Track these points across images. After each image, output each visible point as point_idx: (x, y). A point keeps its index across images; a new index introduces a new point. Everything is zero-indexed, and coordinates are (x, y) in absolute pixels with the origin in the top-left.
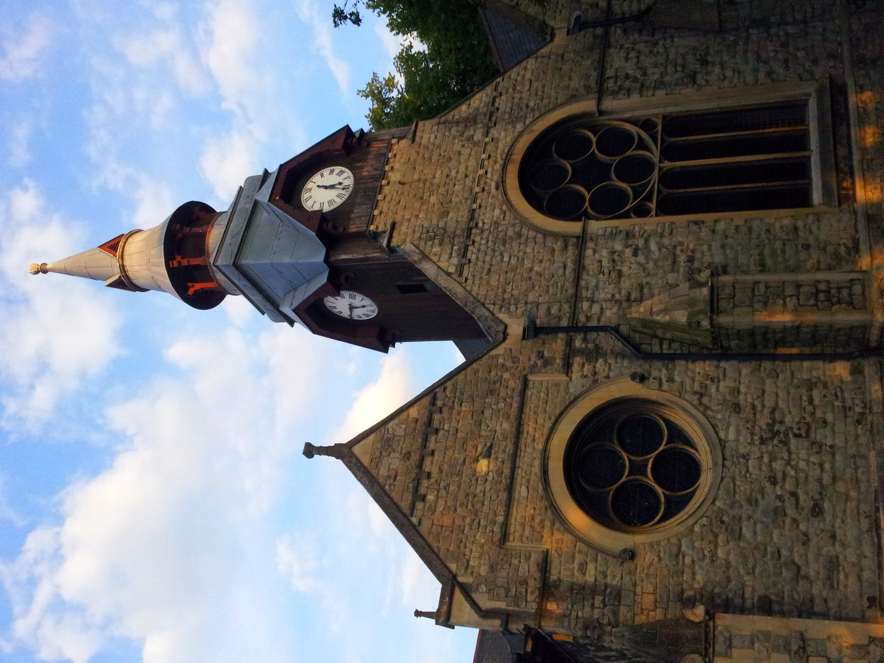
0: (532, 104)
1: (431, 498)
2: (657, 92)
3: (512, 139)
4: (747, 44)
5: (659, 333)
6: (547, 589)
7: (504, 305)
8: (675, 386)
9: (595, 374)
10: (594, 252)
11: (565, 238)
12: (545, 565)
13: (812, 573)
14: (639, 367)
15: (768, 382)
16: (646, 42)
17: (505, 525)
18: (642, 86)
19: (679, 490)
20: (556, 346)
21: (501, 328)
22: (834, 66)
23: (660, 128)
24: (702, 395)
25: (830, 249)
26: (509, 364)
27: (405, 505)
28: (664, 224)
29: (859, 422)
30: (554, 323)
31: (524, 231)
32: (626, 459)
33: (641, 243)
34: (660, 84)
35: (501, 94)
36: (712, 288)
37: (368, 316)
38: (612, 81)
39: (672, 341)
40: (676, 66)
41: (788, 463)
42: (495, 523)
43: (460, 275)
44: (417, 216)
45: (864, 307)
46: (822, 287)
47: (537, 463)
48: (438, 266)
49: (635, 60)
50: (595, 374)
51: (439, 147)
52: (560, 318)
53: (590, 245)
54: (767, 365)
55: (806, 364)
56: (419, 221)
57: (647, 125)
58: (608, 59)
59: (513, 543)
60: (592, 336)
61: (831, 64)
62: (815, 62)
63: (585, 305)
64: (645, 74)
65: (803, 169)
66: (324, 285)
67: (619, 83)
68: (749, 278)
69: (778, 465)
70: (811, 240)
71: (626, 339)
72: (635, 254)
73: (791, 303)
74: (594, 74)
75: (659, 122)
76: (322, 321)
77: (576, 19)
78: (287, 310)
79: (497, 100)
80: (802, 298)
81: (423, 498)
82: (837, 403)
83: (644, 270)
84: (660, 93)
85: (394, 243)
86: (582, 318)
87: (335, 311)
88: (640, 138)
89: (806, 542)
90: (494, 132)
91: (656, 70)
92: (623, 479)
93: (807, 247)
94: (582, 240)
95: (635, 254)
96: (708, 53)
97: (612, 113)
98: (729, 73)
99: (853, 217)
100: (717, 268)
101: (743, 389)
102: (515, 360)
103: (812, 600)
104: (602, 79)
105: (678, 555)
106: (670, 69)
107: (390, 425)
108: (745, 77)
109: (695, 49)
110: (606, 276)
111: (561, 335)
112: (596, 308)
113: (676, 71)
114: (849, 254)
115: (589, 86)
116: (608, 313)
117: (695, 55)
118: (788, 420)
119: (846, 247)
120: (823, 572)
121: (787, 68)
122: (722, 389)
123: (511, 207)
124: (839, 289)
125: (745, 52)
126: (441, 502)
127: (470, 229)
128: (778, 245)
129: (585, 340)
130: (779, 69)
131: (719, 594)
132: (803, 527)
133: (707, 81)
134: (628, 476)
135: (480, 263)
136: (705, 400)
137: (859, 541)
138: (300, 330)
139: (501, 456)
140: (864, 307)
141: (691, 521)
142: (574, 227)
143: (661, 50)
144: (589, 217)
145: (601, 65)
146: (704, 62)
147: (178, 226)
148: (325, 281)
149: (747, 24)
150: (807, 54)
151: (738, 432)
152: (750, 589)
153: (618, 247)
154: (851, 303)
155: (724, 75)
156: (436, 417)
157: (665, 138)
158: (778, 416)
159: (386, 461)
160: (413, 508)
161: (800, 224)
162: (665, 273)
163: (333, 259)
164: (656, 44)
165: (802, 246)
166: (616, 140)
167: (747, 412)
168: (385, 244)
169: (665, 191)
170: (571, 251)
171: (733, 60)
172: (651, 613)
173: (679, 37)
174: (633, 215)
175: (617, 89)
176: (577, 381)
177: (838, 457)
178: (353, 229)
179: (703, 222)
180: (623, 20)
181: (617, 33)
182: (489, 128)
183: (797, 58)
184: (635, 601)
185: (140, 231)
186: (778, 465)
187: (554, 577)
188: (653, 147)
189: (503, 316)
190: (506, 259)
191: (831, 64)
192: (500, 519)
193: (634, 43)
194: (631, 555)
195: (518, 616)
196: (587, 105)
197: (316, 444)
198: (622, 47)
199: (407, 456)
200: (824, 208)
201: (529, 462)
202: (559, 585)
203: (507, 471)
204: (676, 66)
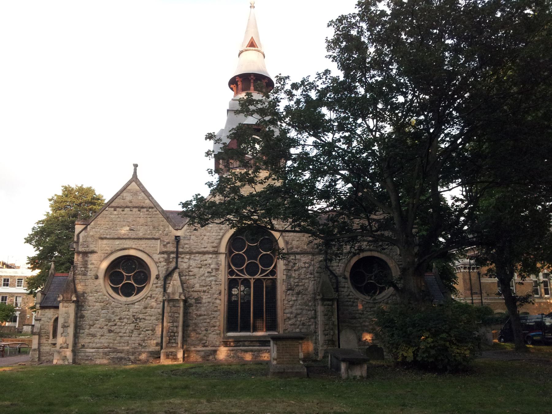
1: (115, 212)
6: (85, 254)
8: (154, 289)
9: (160, 262)
10: (211, 258)
11: (218, 246)
12: (93, 252)
13: (91, 330)
14: (162, 276)
15: (155, 318)
17: (106, 238)
20: (171, 248)
23: (271, 277)
24: (151, 297)
25: (205, 338)
26: (165, 232)
27: (113, 204)
29: (139, 344)
30: (180, 246)
31: (223, 231)
33: (213, 274)
34: (289, 277)
38: (294, 258)
41: (126, 323)
42: (107, 235)
46: (176, 334)
47: (127, 246)
50: (160, 262)
52: (183, 248)
53: (214, 256)
57: (273, 272)
59: (100, 242)
60: (175, 260)
63: (188, 257)
64: (295, 271)
69: (125, 320)
70: (209, 332)
72: (208, 272)
73: (170, 325)
75: (274, 277)
80: (172, 328)
81: (115, 210)
82: (146, 338)
84: (285, 277)
86: (183, 256)
88: (267, 270)
93: (207, 330)
94: (216, 253)
95: (208, 272)
98: (291, 303)
101: (152, 310)
102: (167, 235)
103: (83, 329)
105: (97, 292)
106: (296, 280)
107: (143, 194)
109: (307, 289)
111: (175, 250)
112: (186, 260)
116: (184, 265)
118: (140, 323)
120: (91, 333)
121: (291, 325)
122: (153, 303)
126: (113, 216)
128: (208, 320)
129: (173, 258)
132: (105, 327)
133: (289, 294)
136: (149, 298)
137: (101, 343)
139: (130, 234)
141: (107, 295)
142: (223, 248)
143: (307, 277)
146: (298, 293)
151: (137, 308)
153: (212, 266)
154: (169, 343)
156: (145, 210)
159: (129, 195)
160: (112, 207)
161: (216, 328)
164: (311, 274)
166: (268, 261)
167: (144, 311)
170: (211, 249)
176: (156, 257)
177: (128, 338)
186: (125, 320)
187: (89, 255)
192: (108, 237)
194: (97, 278)
195: (78, 246)
199: (131, 202)
203: (125, 237)
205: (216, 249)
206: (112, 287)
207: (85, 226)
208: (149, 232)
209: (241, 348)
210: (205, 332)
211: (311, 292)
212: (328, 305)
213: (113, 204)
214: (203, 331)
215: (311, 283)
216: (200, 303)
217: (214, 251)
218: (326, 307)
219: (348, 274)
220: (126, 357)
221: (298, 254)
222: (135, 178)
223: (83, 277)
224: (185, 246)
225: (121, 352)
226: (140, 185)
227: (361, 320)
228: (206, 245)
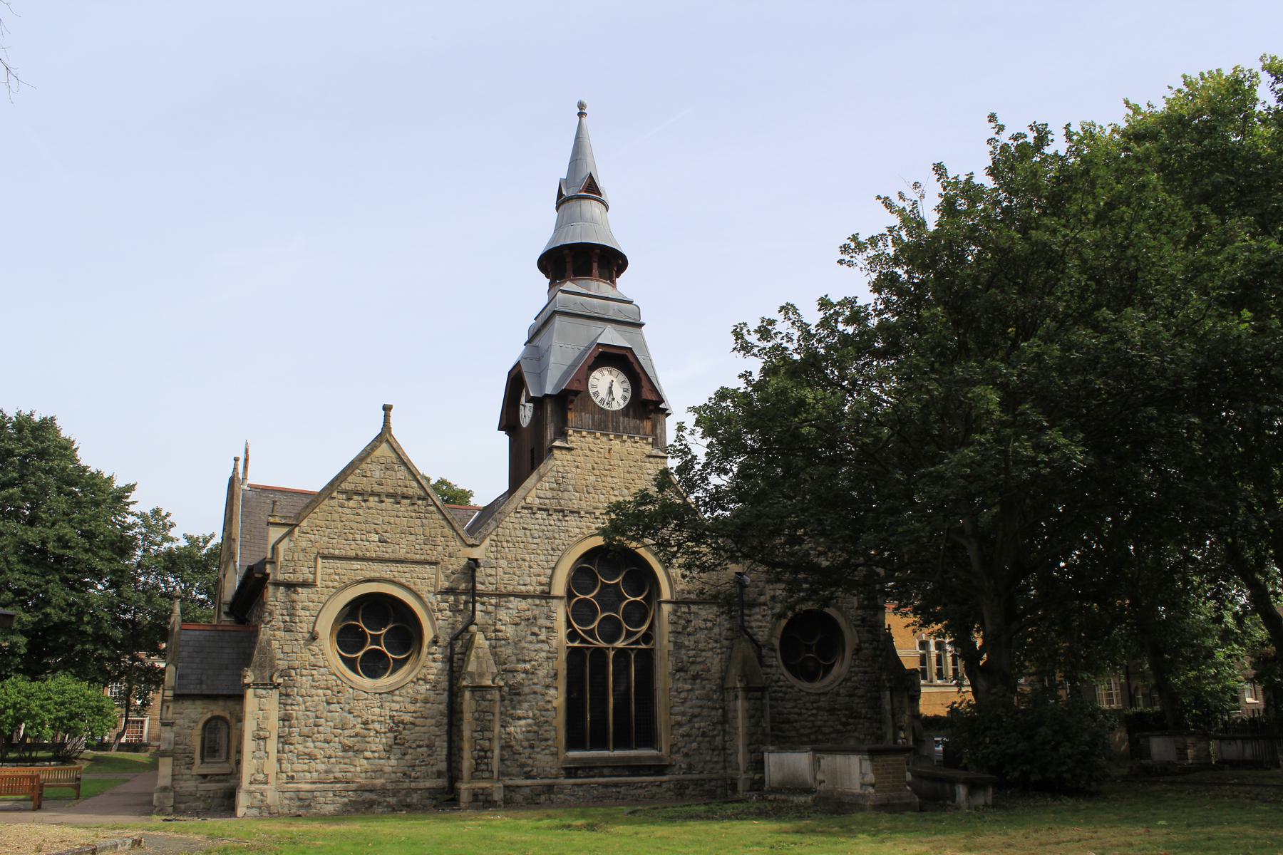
1: (351, 503)
6: (291, 586)
7: (496, 543)
14: (444, 639)
15: (433, 721)
23: (644, 646)
25: (530, 762)
27: (344, 486)
33: (542, 637)
34: (678, 646)
46: (489, 754)
51: (640, 478)
53: (544, 602)
54: (445, 721)
55: (445, 744)
57: (647, 637)
63: (493, 601)
64: (689, 634)
71: (466, 629)
76: (516, 382)
81: (349, 499)
84: (671, 647)
85: (556, 452)
86: (486, 599)
89: (326, 741)
93: (532, 747)
96: (703, 680)
98: (683, 695)
104: (687, 603)
106: (691, 653)
109: (709, 670)
118: (407, 732)
121: (683, 736)
126: (347, 511)
140: (472, 778)
142: (559, 588)
154: (476, 770)
161: (550, 743)
163: (548, 400)
164: (716, 641)
168: (557, 443)
178: (571, 416)
187: (300, 590)
189: (487, 541)
192: (337, 552)
194: (313, 637)
195: (275, 569)
196: (666, 594)
197: (392, 413)
206: (344, 659)
207: (285, 530)
208: (418, 547)
209: (596, 779)
210: (529, 750)
211: (717, 675)
212: (756, 699)
213: (344, 486)
214: (524, 748)
215: (717, 659)
216: (518, 694)
217: (543, 592)
219: (776, 642)
221: (694, 603)
222: (385, 435)
223: (288, 635)
225: (371, 791)
226: (395, 449)
227: (798, 725)
228: (528, 580)
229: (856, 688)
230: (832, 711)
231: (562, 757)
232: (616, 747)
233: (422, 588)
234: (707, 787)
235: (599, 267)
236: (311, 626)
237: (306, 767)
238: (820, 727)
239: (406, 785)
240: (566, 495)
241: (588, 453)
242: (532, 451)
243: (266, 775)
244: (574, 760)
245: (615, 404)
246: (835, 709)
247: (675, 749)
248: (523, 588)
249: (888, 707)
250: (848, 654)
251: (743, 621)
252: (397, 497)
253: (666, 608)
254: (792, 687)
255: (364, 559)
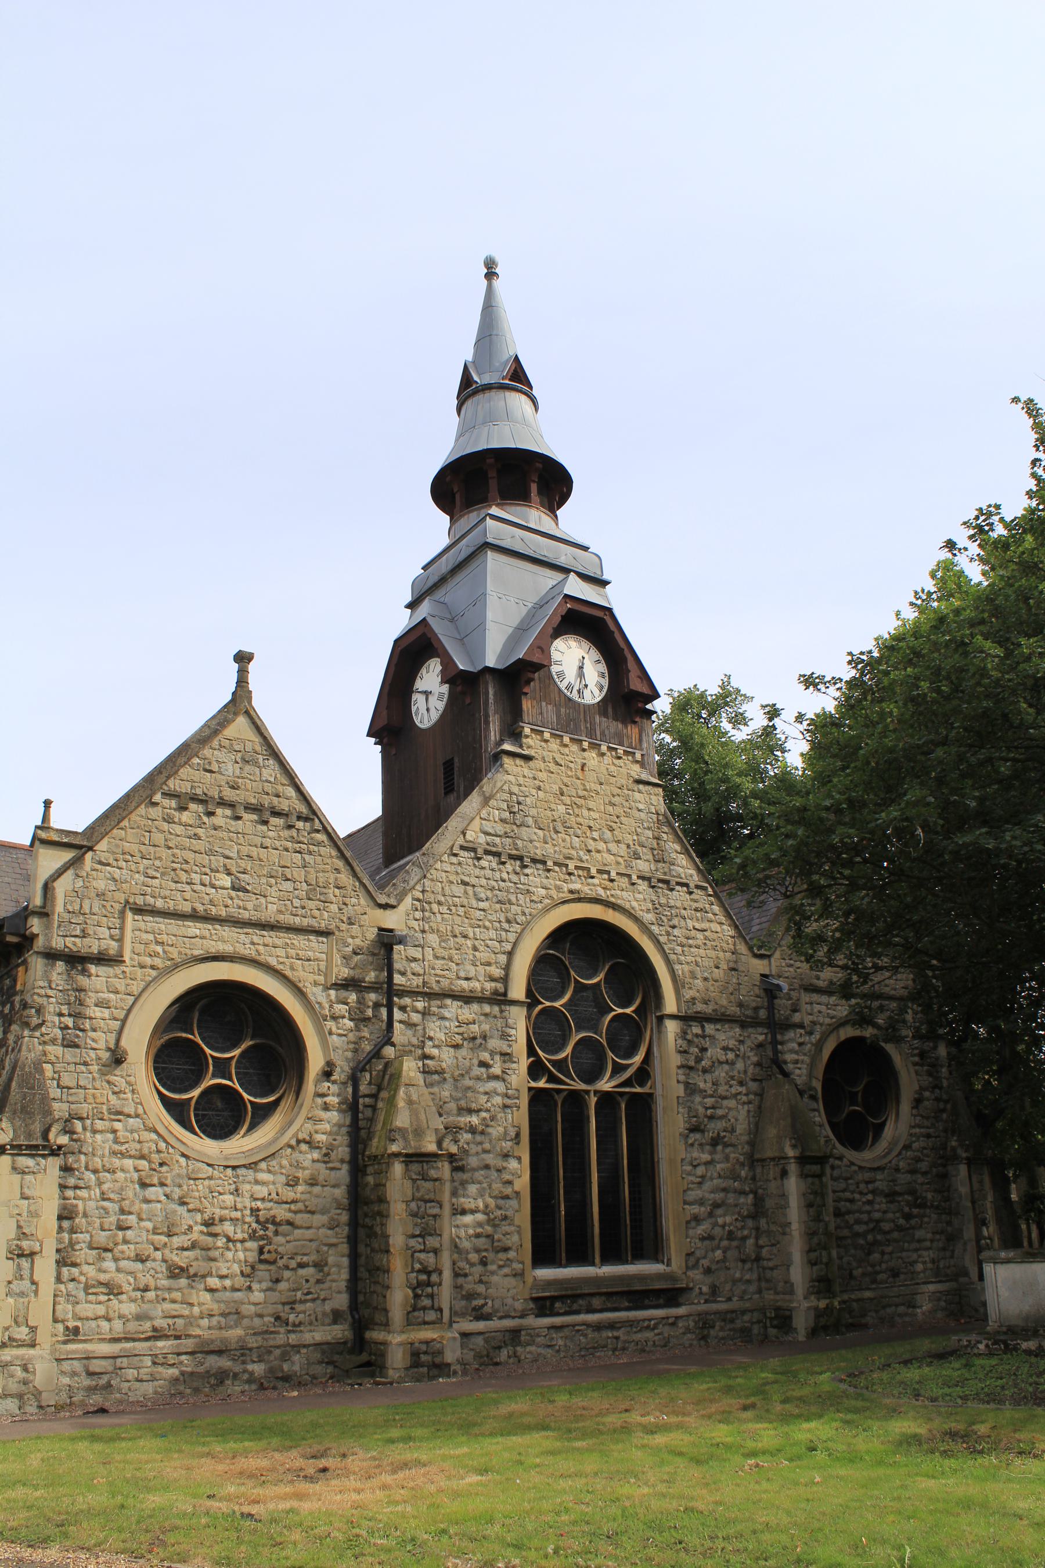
0: (676, 932)
1: (185, 816)
2: (681, 1087)
3: (633, 909)
4: (735, 1191)
5: (384, 1094)
7: (422, 904)
15: (324, 1219)
16: (745, 1072)
18: (691, 1068)
19: (196, 1116)
21: (392, 901)
22: (701, 1293)
23: (638, 1090)
28: (518, 1098)
29: (278, 1318)
32: (232, 1054)
33: (496, 1070)
34: (691, 1089)
35: (691, 893)
36: (435, 1155)
37: (417, 713)
39: (374, 1108)
40: (713, 1108)
43: (462, 848)
44: (539, 788)
45: (410, 1322)
46: (434, 1278)
48: (474, 819)
49: (723, 1058)
52: (403, 974)
53: (496, 1009)
54: (345, 1217)
55: (345, 1261)
56: (534, 792)
57: (643, 1074)
58: (726, 1026)
61: (705, 1289)
62: (708, 1271)
63: (420, 1005)
64: (705, 1071)
65: (579, 1255)
66: (457, 667)
67: (695, 1040)
68: (446, 1196)
70: (492, 1267)
71: (377, 1054)
74: (708, 1009)
76: (411, 653)
77: (778, 985)
78: (425, 610)
79: (685, 889)
80: (422, 1256)
82: (299, 1294)
83: (462, 1075)
84: (680, 1090)
85: (507, 761)
87: (423, 671)
88: (626, 1067)
89: (140, 1259)
90: (643, 886)
91: (709, 1085)
92: (208, 1051)
93: (484, 1263)
96: (726, 1145)
97: (659, 1032)
98: (700, 1171)
99: (518, 1314)
100: (461, 1160)
101: (317, 1189)
106: (709, 1101)
108: (692, 1190)
109: (733, 1130)
110: (456, 1030)
113: (707, 1108)
114: (474, 1309)
115: (694, 1004)
117: (724, 1131)
118: (280, 1239)
119: (483, 1306)
121: (703, 1239)
123: (547, 910)
124: (431, 1296)
125: (724, 1190)
126: (179, 829)
127: (520, 858)
130: (702, 1229)
131: (78, 1161)
133: (692, 1145)
134: (212, 1056)
135: (477, 871)
138: (401, 621)
140: (410, 1322)
143: (733, 1090)
144: (530, 1007)
145: (720, 1018)
146: (715, 1142)
147: (539, 465)
148: (461, 668)
149: (760, 1191)
150: (718, 1262)
152: (87, 1196)
154: (415, 1308)
155: (699, 1165)
157: (626, 1097)
158: (285, 1228)
161: (512, 1254)
162: (457, 1100)
163: (488, 677)
164: (741, 1083)
165: (485, 1257)
168: (507, 747)
169: (559, 1099)
171: (715, 1175)
172: (55, 1082)
173: (749, 1111)
174: (532, 1059)
175: (689, 1037)
178: (526, 704)
179: (518, 1143)
180: (775, 1043)
181: (759, 1036)
182: (649, 879)
183: (713, 1250)
184: (68, 1064)
185: (537, 409)
187: (93, 968)
188: (613, 1083)
189: (408, 901)
190: (482, 905)
191: (705, 1289)
192: (160, 904)
193: (745, 1057)
195: (48, 927)
197: (251, 667)
198: (741, 1042)
200: (530, 1280)
201: (229, 940)
202: (84, 975)
204: (713, 1108)
205: (500, 986)
207: (67, 855)
210: (478, 1269)
211: (745, 1138)
212: (814, 1176)
213: (173, 784)
214: (472, 1265)
215: (743, 1111)
217: (496, 992)
218: (810, 1180)
219: (818, 1085)
220: (238, 1368)
223: (70, 1054)
224: (410, 967)
225: (219, 1352)
229: (918, 1160)
230: (891, 1196)
231: (530, 1280)
232: (606, 1260)
233: (304, 976)
234: (738, 1324)
235: (540, 492)
236: (112, 1039)
237: (101, 1310)
238: (878, 1221)
239: (280, 1339)
240: (524, 832)
241: (553, 767)
242: (449, 766)
243: (33, 1329)
244: (550, 1283)
245: (587, 693)
246: (895, 1193)
247: (692, 1260)
248: (465, 984)
249: (964, 1190)
250: (905, 1107)
251: (776, 1052)
252: (264, 813)
253: (672, 1027)
254: (840, 1158)
255: (206, 918)
